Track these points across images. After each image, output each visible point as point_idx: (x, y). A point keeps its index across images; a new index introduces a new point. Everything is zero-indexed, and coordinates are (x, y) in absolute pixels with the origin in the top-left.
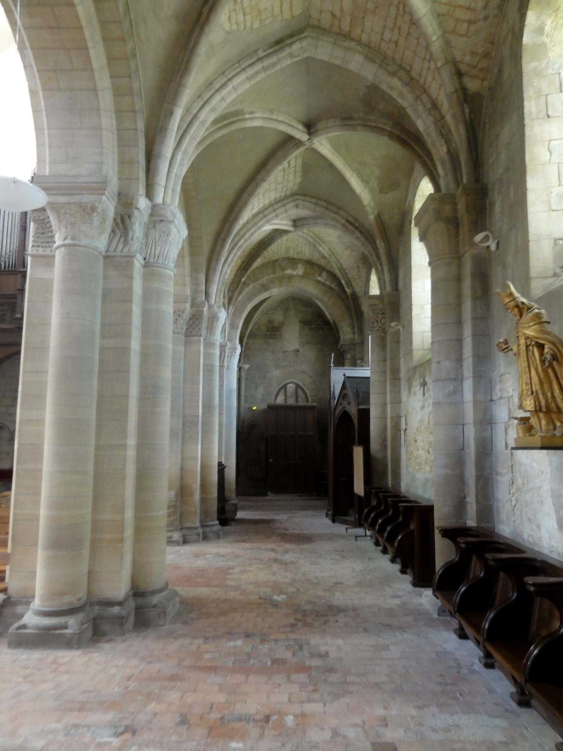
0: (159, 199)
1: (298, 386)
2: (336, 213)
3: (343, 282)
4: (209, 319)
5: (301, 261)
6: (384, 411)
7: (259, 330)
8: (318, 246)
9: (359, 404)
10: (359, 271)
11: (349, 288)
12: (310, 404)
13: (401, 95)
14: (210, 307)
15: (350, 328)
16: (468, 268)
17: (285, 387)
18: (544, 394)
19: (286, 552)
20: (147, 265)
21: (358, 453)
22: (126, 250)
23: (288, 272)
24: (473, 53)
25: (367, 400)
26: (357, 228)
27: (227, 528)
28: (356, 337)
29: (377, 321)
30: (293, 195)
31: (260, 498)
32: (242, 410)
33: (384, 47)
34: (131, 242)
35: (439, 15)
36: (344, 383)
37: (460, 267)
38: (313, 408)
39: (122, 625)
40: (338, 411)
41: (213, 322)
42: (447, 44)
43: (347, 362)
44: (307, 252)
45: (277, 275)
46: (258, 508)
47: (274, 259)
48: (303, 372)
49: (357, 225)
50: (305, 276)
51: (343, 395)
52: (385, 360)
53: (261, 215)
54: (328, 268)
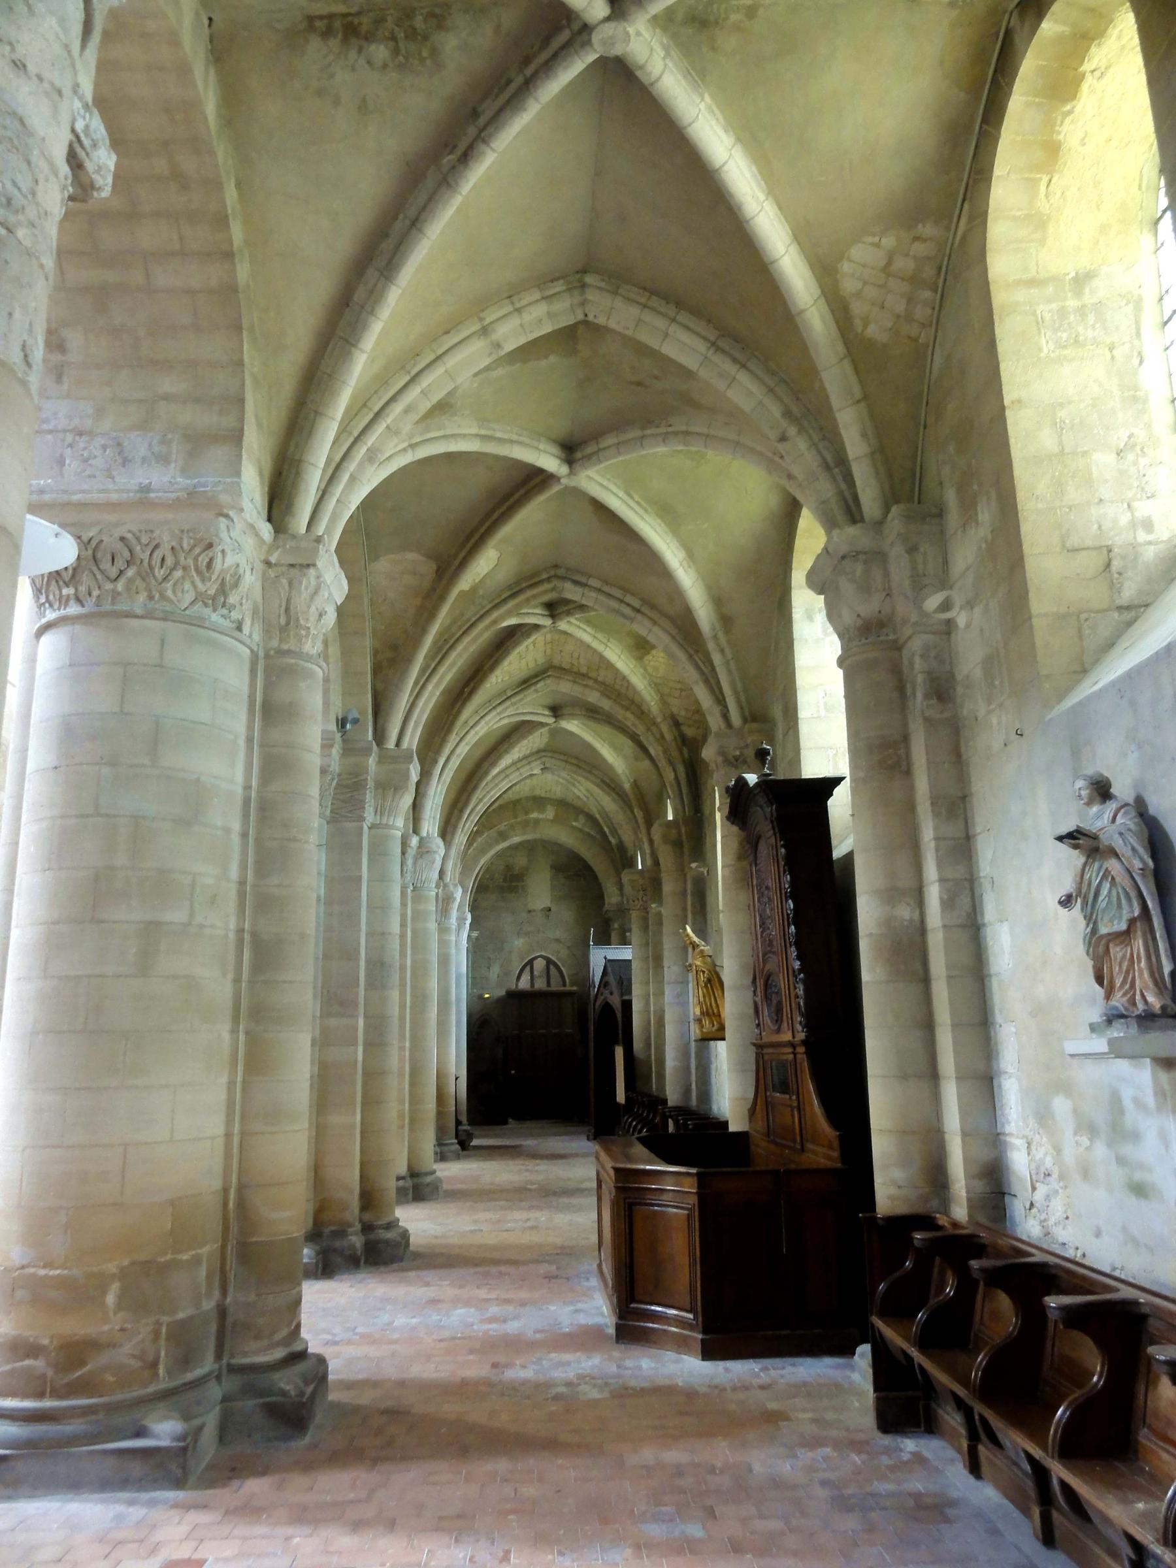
0: (424, 834)
1: (549, 962)
3: (606, 829)
4: (443, 900)
5: (549, 799)
6: (647, 1003)
8: (573, 789)
9: (622, 995)
11: (613, 837)
12: (568, 988)
14: (445, 886)
16: (689, 887)
18: (706, 1004)
19: (538, 1165)
20: (415, 889)
21: (619, 1052)
23: (534, 815)
24: (687, 710)
25: (629, 991)
27: (465, 1152)
30: (538, 751)
31: (500, 1127)
33: (617, 687)
35: (656, 684)
36: (605, 967)
37: (685, 882)
39: (407, 1195)
40: (598, 1004)
42: (663, 701)
43: (614, 936)
44: (558, 792)
45: (519, 819)
46: (497, 1136)
48: (557, 940)
50: (556, 820)
51: (604, 983)
52: (647, 944)
53: (503, 775)
54: (586, 810)
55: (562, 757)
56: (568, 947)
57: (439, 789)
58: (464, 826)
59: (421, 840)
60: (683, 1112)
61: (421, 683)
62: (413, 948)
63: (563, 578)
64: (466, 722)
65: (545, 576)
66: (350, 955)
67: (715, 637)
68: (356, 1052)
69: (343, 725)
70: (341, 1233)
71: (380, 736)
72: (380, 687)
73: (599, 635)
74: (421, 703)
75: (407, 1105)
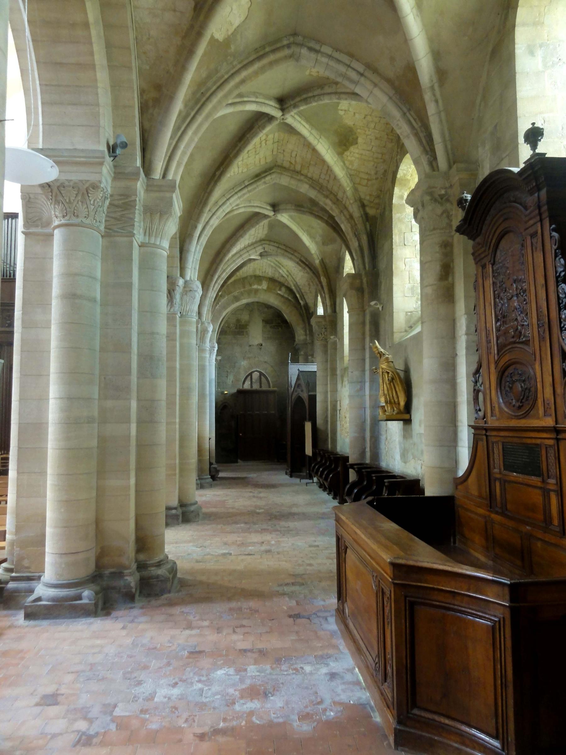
0: (188, 278)
1: (261, 374)
2: (292, 254)
3: (298, 295)
6: (326, 397)
7: (229, 327)
8: (279, 269)
9: (309, 391)
11: (302, 300)
12: (271, 389)
13: (331, 209)
14: (203, 323)
16: (368, 318)
17: (251, 374)
18: (389, 395)
19: (260, 492)
21: (308, 426)
22: (172, 310)
24: (370, 195)
25: (314, 388)
26: (307, 265)
27: (215, 482)
28: (308, 338)
29: (322, 334)
30: (261, 240)
31: (233, 464)
33: (321, 181)
34: (175, 305)
35: (350, 175)
37: (364, 316)
38: (273, 392)
39: (178, 519)
40: (293, 398)
41: (204, 334)
42: (356, 190)
43: (301, 358)
44: (270, 273)
45: (246, 289)
46: (233, 471)
49: (307, 263)
50: (269, 290)
51: (298, 385)
52: (327, 361)
53: (238, 255)
54: (286, 284)
55: (275, 244)
57: (198, 249)
58: (214, 286)
59: (186, 282)
60: (360, 468)
61: (183, 129)
62: (181, 356)
63: (301, 45)
64: (216, 202)
65: (285, 42)
66: (125, 349)
67: (432, 88)
68: (129, 429)
69: (114, 150)
70: (119, 575)
71: (147, 166)
72: (147, 125)
73: (314, 132)
74: (182, 146)
75: (177, 461)
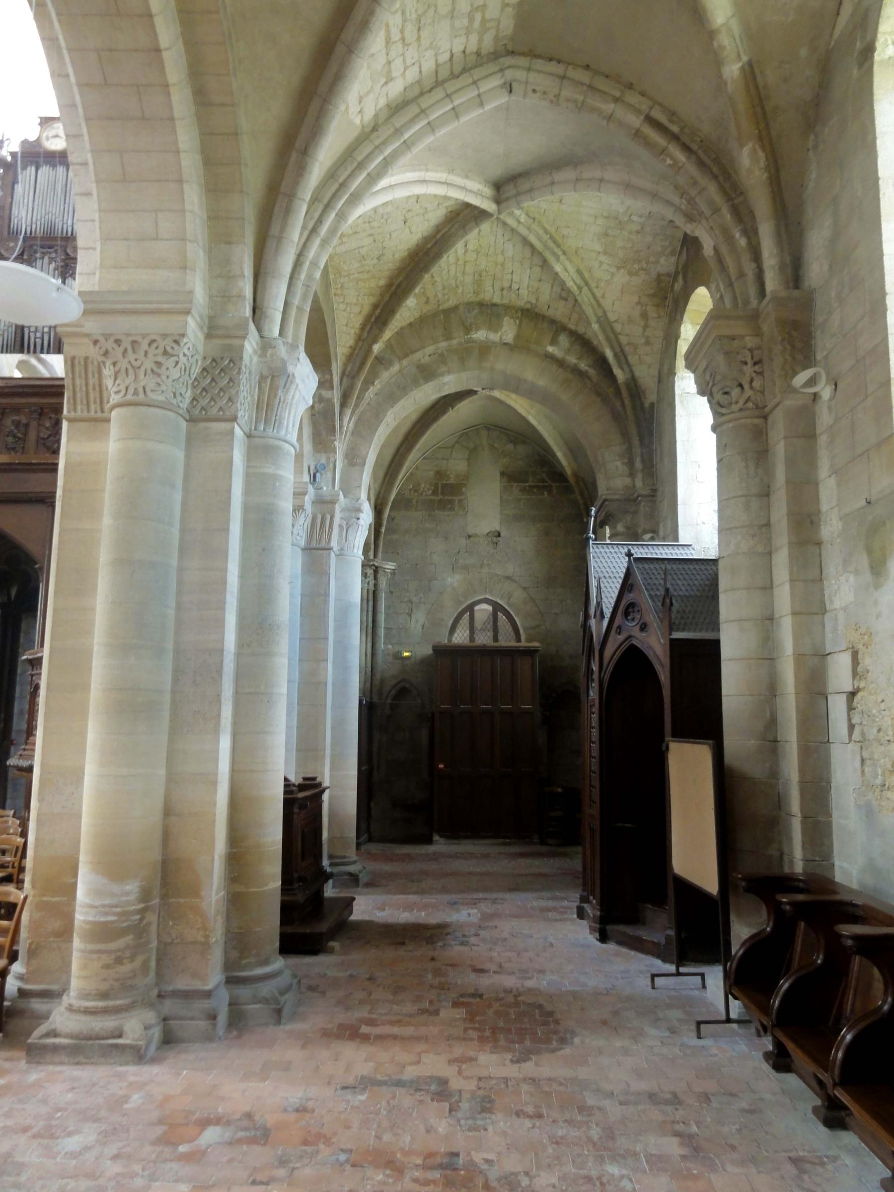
1: (497, 607)
2: (616, 100)
3: (609, 354)
5: (508, 309)
7: (416, 491)
10: (646, 327)
12: (524, 643)
15: (623, 463)
17: (470, 608)
23: (481, 335)
26: (675, 138)
28: (639, 483)
29: (741, 385)
32: (380, 658)
36: (628, 574)
40: (608, 653)
41: (273, 389)
45: (455, 342)
47: (446, 306)
49: (675, 129)
50: (518, 346)
52: (766, 493)
53: (413, 110)
55: (553, 67)
56: (525, 588)
